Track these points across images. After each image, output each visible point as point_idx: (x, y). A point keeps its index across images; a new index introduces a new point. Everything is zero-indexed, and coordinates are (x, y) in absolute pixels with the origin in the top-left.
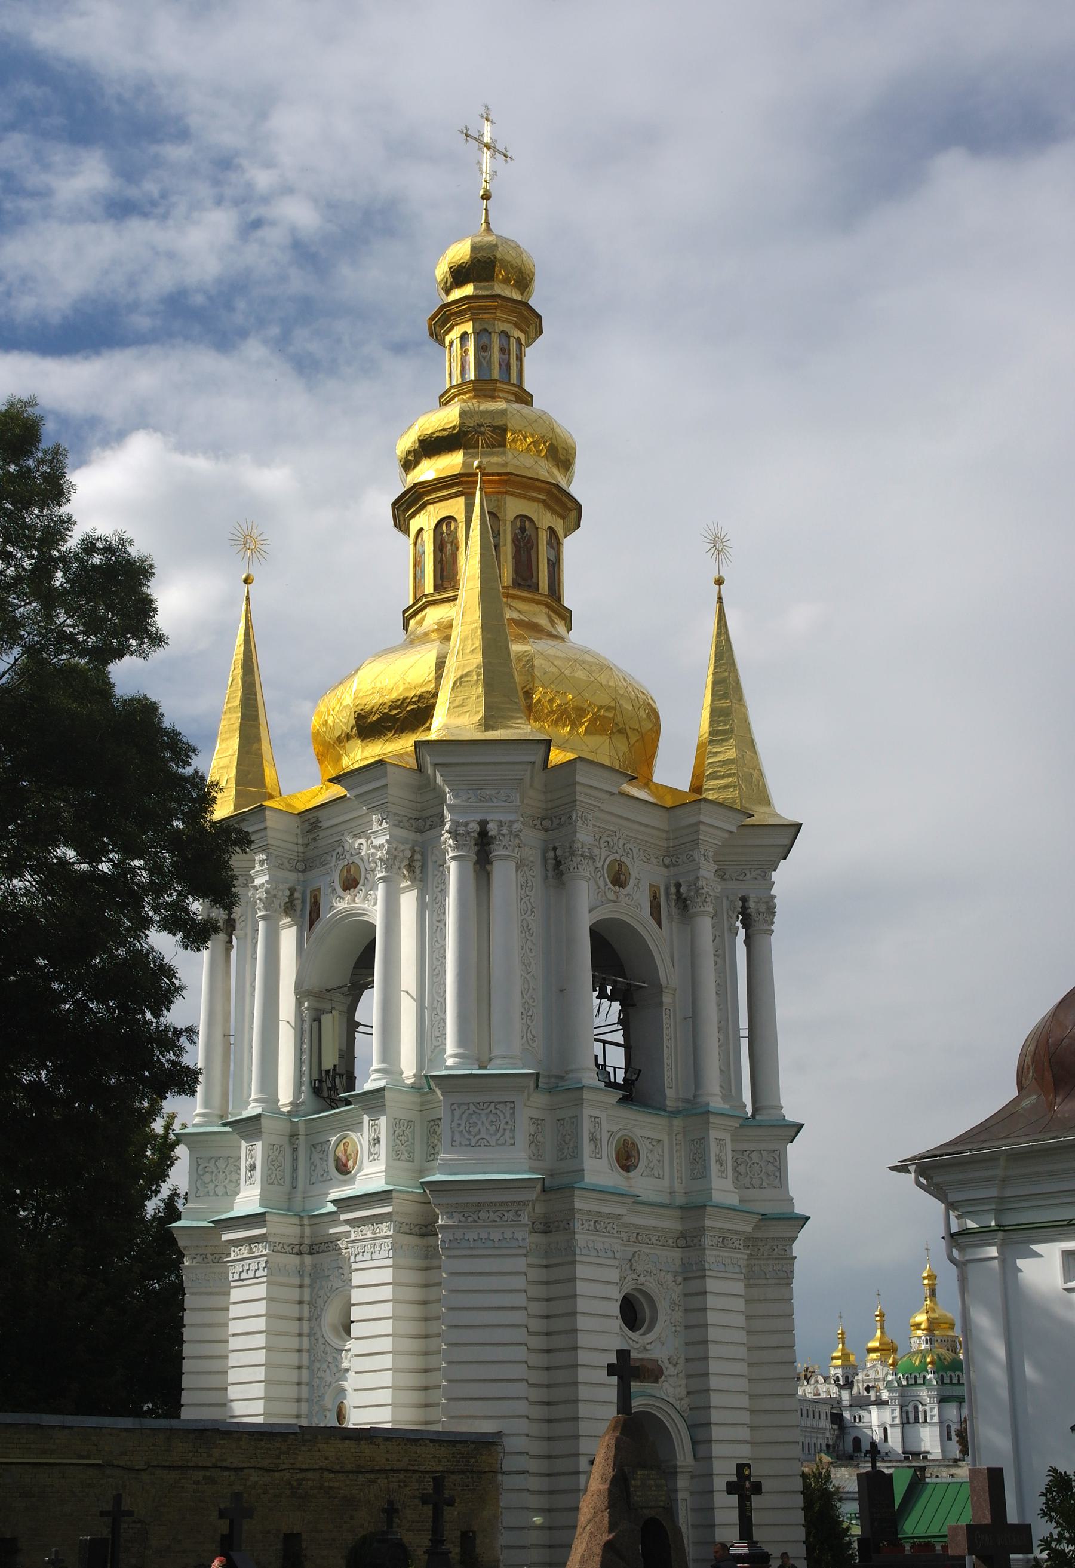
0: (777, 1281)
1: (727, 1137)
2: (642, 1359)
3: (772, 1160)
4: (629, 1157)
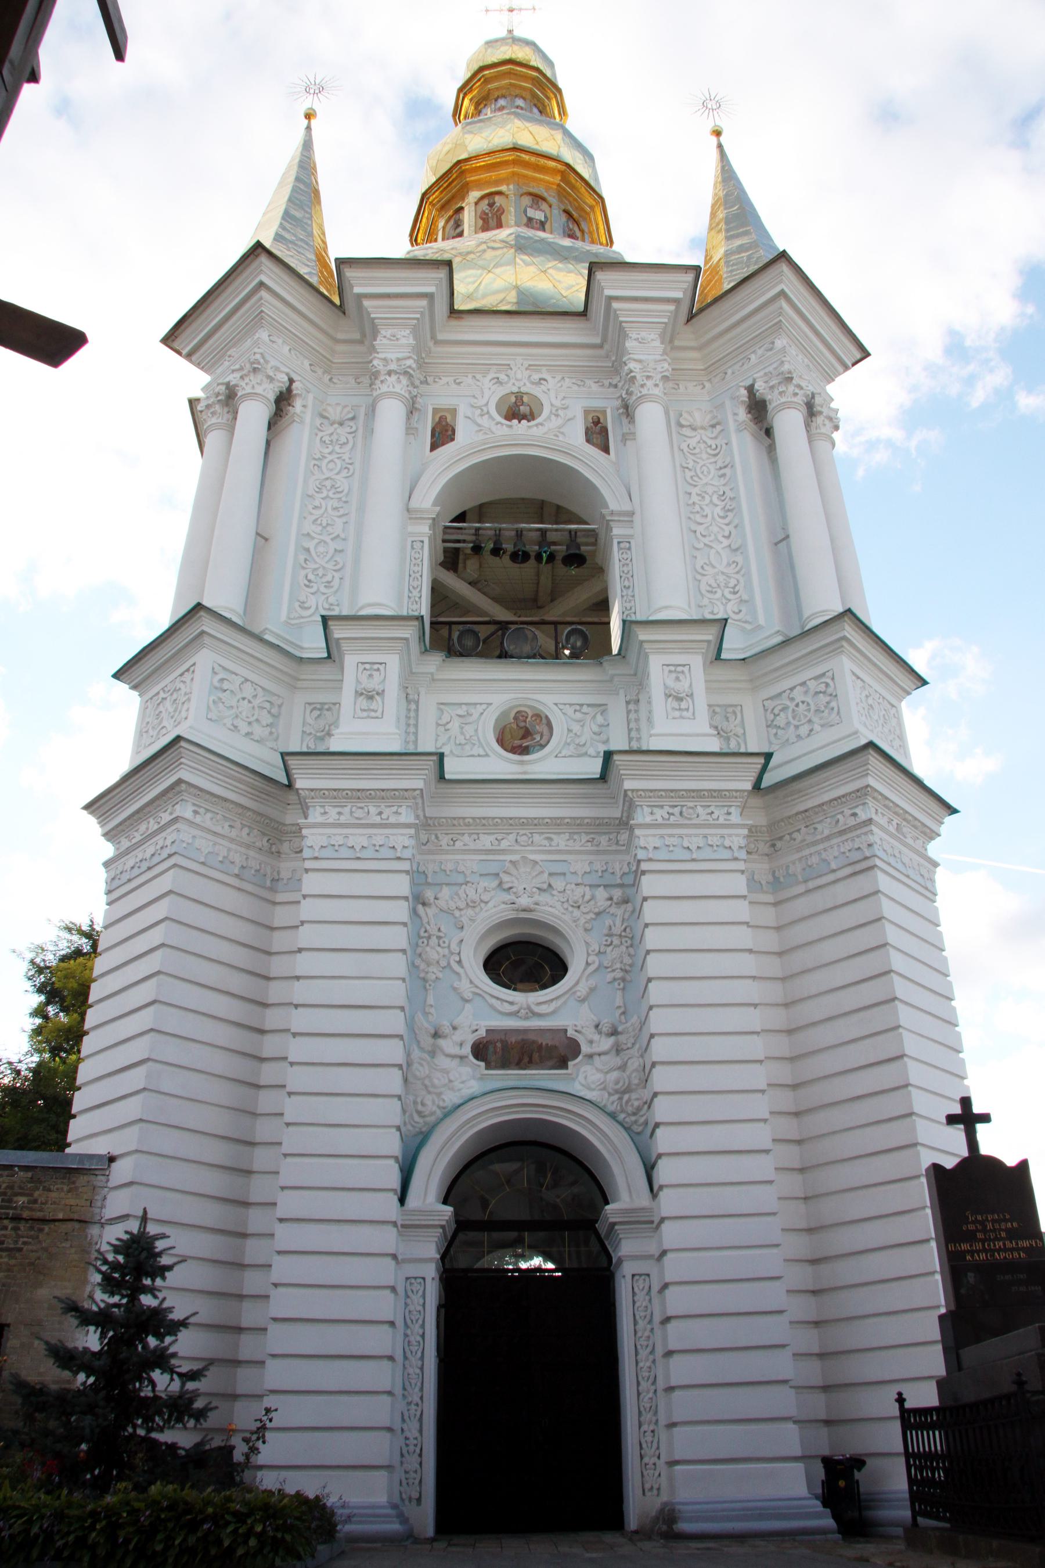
0: (848, 871)
2: (526, 1031)
3: (822, 687)
4: (527, 734)
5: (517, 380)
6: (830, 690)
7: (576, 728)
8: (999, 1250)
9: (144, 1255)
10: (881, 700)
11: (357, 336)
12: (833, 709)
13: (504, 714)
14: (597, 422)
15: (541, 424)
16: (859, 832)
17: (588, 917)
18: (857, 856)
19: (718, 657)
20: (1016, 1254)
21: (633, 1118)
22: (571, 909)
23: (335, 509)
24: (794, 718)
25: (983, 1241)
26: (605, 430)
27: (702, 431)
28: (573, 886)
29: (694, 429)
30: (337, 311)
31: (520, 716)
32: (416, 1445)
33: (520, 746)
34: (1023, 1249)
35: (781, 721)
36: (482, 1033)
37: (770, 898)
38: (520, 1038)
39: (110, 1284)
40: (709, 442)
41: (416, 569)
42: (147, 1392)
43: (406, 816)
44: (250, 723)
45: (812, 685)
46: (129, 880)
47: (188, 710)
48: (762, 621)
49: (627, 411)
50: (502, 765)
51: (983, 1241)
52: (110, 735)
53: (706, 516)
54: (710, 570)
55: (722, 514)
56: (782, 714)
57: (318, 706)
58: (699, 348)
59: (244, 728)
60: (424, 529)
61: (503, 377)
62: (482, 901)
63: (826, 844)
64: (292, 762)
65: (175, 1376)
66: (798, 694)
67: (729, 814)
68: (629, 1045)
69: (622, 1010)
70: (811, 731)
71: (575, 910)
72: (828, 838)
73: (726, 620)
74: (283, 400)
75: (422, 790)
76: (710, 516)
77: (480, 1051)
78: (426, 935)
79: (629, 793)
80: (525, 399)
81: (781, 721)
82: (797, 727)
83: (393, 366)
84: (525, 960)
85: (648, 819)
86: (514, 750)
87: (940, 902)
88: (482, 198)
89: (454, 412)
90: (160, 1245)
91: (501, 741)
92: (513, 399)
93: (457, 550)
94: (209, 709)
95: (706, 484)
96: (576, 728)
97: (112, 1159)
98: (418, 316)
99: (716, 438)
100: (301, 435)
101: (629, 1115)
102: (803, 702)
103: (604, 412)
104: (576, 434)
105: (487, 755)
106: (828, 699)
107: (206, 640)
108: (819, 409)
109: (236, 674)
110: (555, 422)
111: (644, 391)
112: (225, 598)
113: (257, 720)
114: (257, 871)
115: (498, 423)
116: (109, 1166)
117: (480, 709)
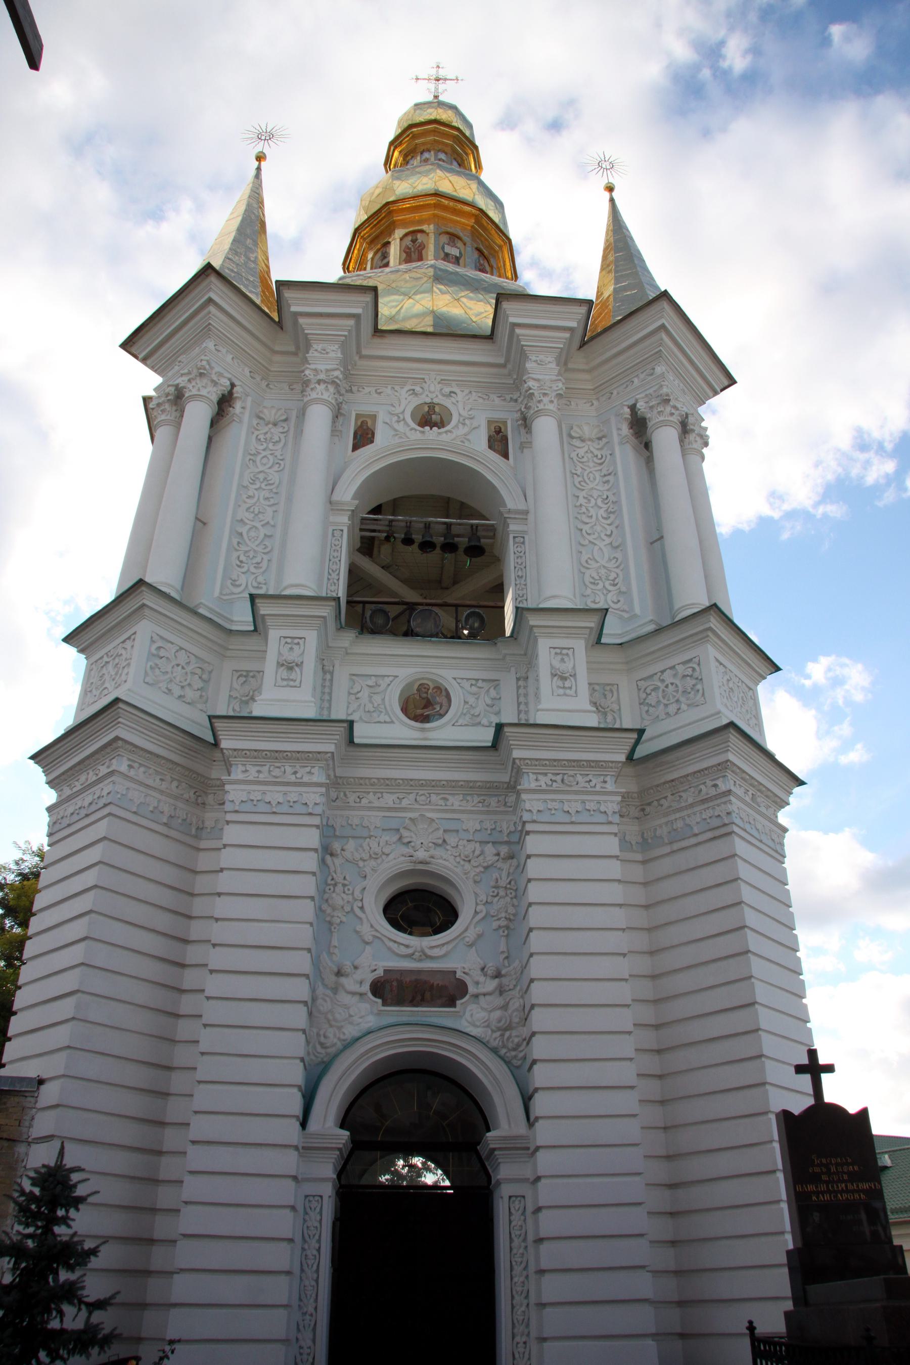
0: (709, 835)
2: (419, 972)
3: (689, 672)
4: (428, 704)
5: (430, 392)
6: (696, 674)
7: (471, 700)
8: (842, 1192)
9: (59, 1187)
10: (740, 684)
11: (292, 348)
12: (698, 691)
13: (409, 686)
14: (498, 431)
15: (450, 431)
16: (719, 801)
17: (478, 870)
18: (716, 822)
19: (598, 641)
20: (856, 1196)
21: (513, 1053)
22: (462, 863)
23: (267, 499)
24: (664, 698)
25: (827, 1183)
26: (505, 439)
27: (589, 443)
28: (465, 842)
29: (583, 441)
30: (275, 326)
31: (423, 688)
32: (309, 1354)
33: (422, 715)
34: (863, 1191)
35: (652, 700)
36: (380, 972)
37: (639, 857)
38: (413, 978)
39: (26, 1214)
40: (596, 452)
41: (336, 554)
42: (55, 1324)
43: (318, 776)
44: (182, 687)
45: (680, 669)
46: (69, 825)
47: (127, 674)
48: (637, 611)
49: (526, 423)
50: (404, 731)
51: (827, 1183)
52: (56, 691)
53: (591, 517)
54: (593, 565)
55: (605, 516)
56: (653, 693)
57: (244, 674)
58: (589, 371)
59: (177, 691)
60: (344, 520)
61: (418, 389)
62: (384, 853)
63: (689, 811)
64: (218, 724)
65: (83, 1307)
66: (668, 677)
67: (605, 782)
68: (511, 987)
69: (506, 955)
70: (679, 709)
71: (467, 864)
72: (692, 805)
73: (607, 610)
74: (225, 402)
75: (333, 753)
76: (594, 517)
77: (378, 989)
78: (333, 882)
79: (517, 761)
80: (437, 409)
81: (652, 700)
82: (666, 705)
83: (322, 376)
84: (420, 907)
85: (533, 785)
87: (788, 864)
88: (406, 235)
89: (374, 417)
90: (75, 1177)
91: (405, 710)
92: (426, 409)
93: (373, 538)
94: (146, 674)
95: (592, 489)
96: (471, 700)
97: (41, 1082)
98: (346, 333)
99: (601, 449)
100: (239, 433)
101: (509, 1050)
102: (672, 684)
103: (505, 423)
104: (480, 442)
105: (392, 722)
106: (694, 682)
107: (147, 612)
108: (692, 427)
109: (172, 643)
110: (462, 430)
111: (541, 406)
112: (165, 574)
113: (189, 685)
114: (184, 820)
115: (411, 429)
116: (38, 1088)
117: (387, 680)
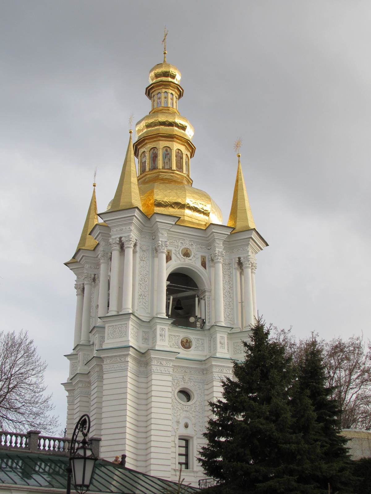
1: (225, 336)
15: (191, 260)
85: (215, 371)
86: (185, 348)
115: (182, 258)
